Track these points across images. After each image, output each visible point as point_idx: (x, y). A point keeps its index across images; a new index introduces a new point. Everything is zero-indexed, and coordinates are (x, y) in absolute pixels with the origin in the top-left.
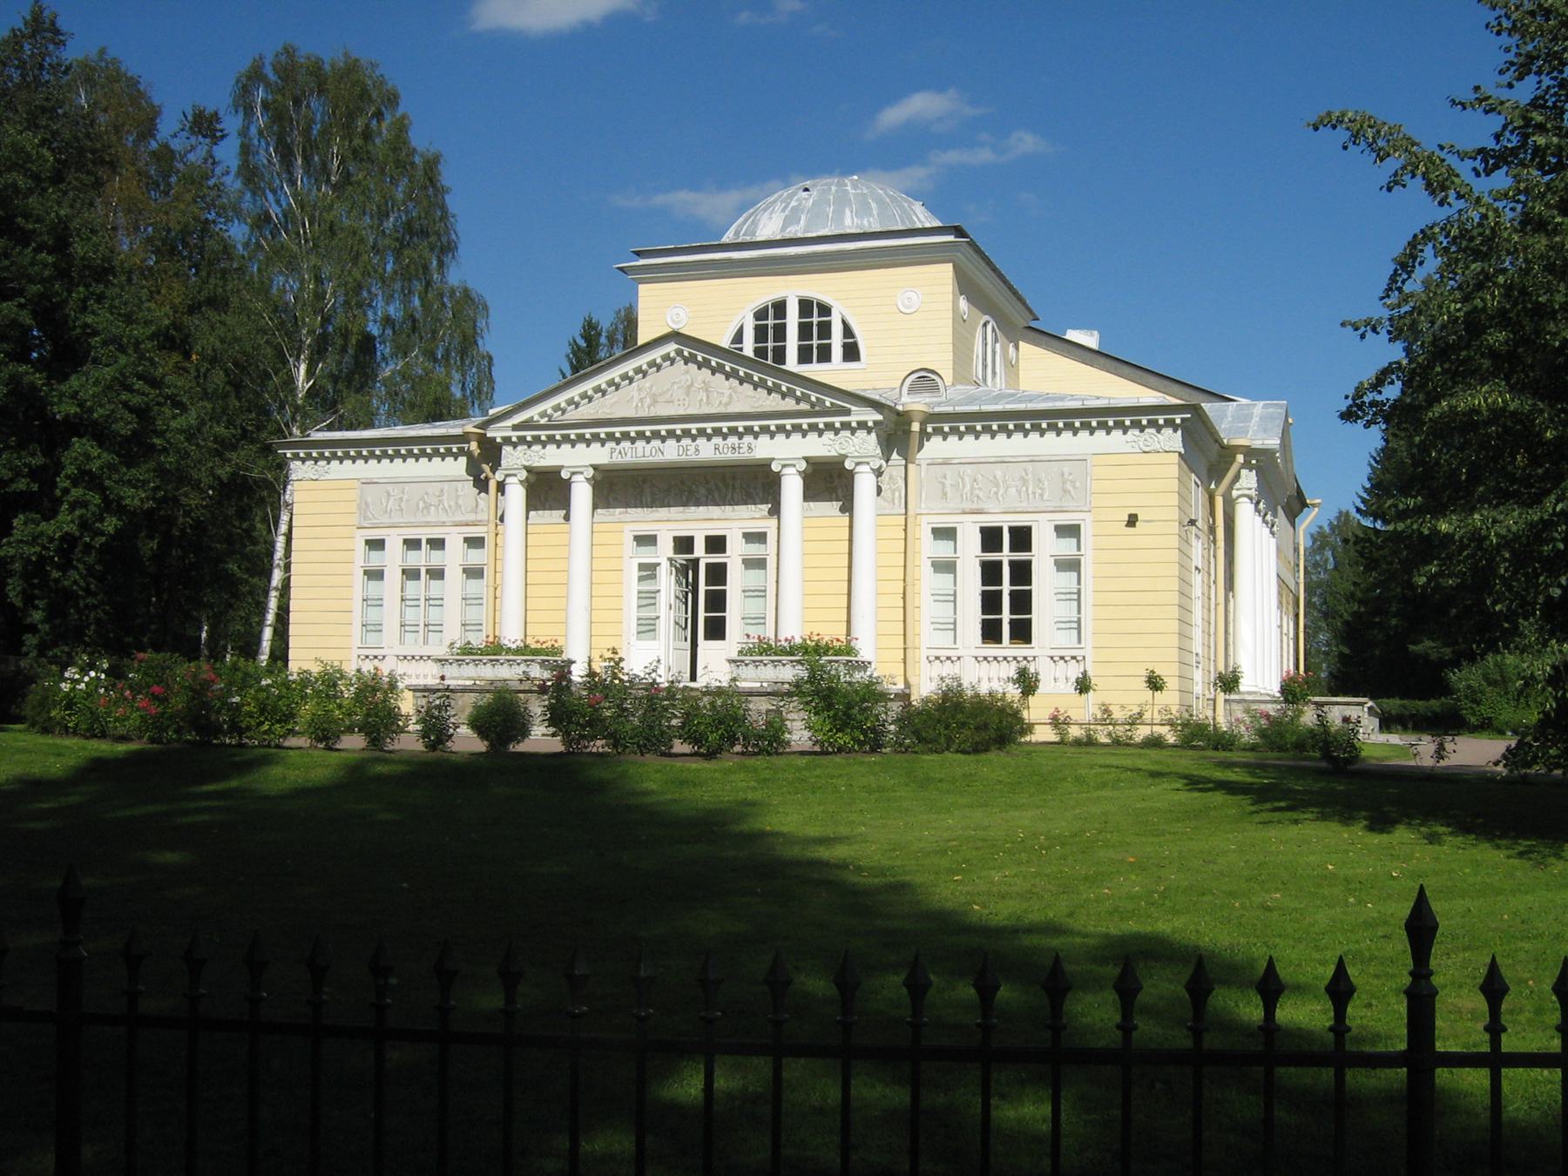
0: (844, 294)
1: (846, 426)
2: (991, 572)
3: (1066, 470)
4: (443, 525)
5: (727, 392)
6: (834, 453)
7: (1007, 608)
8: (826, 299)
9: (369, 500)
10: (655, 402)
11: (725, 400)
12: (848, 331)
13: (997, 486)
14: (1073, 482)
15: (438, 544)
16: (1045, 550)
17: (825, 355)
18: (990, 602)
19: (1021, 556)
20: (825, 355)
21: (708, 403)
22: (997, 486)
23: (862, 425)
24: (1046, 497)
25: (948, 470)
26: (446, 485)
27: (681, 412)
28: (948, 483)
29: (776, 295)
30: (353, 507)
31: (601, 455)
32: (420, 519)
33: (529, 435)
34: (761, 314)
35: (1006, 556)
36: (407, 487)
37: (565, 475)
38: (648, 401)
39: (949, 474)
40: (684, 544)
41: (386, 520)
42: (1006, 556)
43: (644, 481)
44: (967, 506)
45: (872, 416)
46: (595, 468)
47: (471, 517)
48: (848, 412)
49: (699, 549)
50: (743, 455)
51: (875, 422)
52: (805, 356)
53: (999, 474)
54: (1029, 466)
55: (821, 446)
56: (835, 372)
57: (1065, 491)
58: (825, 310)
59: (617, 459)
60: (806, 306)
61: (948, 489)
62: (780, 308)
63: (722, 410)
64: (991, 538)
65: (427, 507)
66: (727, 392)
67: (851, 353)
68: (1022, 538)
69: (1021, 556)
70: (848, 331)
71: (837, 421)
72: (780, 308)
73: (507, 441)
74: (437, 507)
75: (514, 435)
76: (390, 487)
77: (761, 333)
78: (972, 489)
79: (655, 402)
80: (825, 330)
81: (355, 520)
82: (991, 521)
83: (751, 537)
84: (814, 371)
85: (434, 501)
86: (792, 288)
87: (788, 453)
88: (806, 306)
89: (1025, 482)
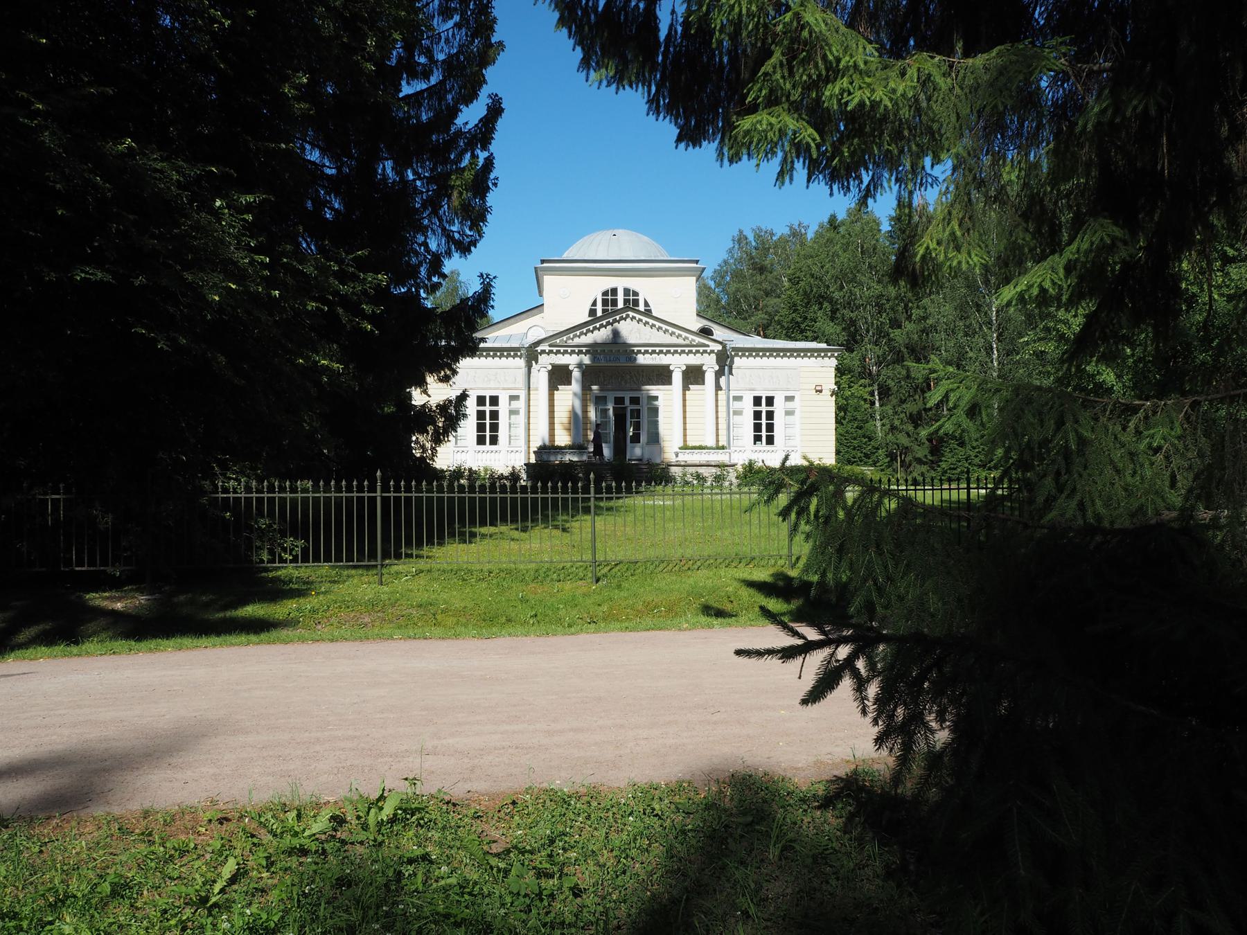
0: (646, 288)
2: (757, 415)
7: (764, 430)
8: (637, 290)
12: (646, 304)
16: (779, 407)
18: (757, 428)
19: (770, 409)
23: (712, 352)
29: (614, 286)
33: (555, 349)
34: (605, 293)
35: (764, 408)
42: (764, 408)
49: (627, 402)
55: (693, 360)
58: (635, 294)
60: (627, 292)
62: (614, 291)
64: (757, 401)
68: (770, 401)
69: (770, 409)
70: (646, 304)
71: (701, 349)
72: (614, 291)
75: (547, 349)
77: (605, 302)
80: (636, 303)
86: (621, 283)
87: (678, 364)
88: (627, 292)
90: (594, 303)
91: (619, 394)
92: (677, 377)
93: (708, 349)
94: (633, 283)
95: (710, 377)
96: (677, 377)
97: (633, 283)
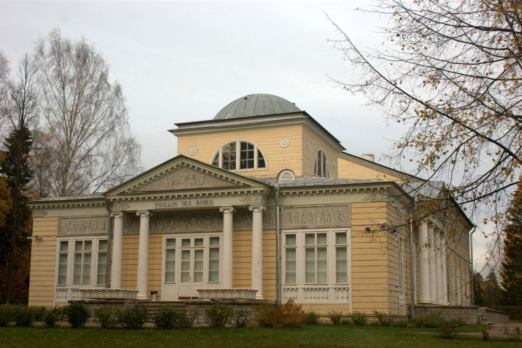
1: (249, 192)
3: (340, 210)
4: (91, 235)
5: (202, 180)
6: (244, 204)
8: (252, 142)
9: (63, 225)
10: (173, 184)
11: (201, 183)
12: (260, 155)
13: (312, 217)
14: (343, 215)
15: (89, 243)
17: (251, 165)
20: (251, 165)
21: (194, 184)
22: (312, 217)
24: (332, 221)
25: (293, 211)
26: (92, 219)
27: (184, 188)
28: (292, 216)
29: (232, 140)
30: (56, 228)
31: (152, 206)
32: (82, 233)
33: (123, 197)
34: (225, 148)
36: (77, 220)
37: (138, 214)
38: (171, 184)
39: (293, 212)
40: (186, 241)
41: (69, 233)
43: (171, 217)
44: (300, 225)
45: (259, 188)
46: (150, 211)
47: (102, 232)
48: (249, 186)
50: (209, 205)
51: (261, 191)
52: (243, 166)
53: (313, 211)
54: (325, 209)
55: (238, 201)
56: (255, 172)
57: (340, 219)
58: (251, 147)
59: (158, 207)
60: (243, 145)
61: (292, 218)
62: (233, 145)
63: (200, 187)
65: (85, 228)
66: (202, 180)
67: (262, 164)
71: (245, 190)
72: (233, 145)
73: (115, 200)
74: (89, 228)
75: (117, 198)
76: (71, 220)
78: (302, 218)
79: (173, 184)
80: (251, 155)
81: (56, 233)
82: (308, 231)
83: (212, 239)
84: (247, 172)
85: (88, 225)
87: (226, 204)
88: (243, 145)
89: (324, 215)
90: (217, 156)
91: (186, 236)
92: (228, 218)
93: (252, 190)
94: (249, 137)
95: (257, 217)
96: (228, 218)
97: (249, 137)
